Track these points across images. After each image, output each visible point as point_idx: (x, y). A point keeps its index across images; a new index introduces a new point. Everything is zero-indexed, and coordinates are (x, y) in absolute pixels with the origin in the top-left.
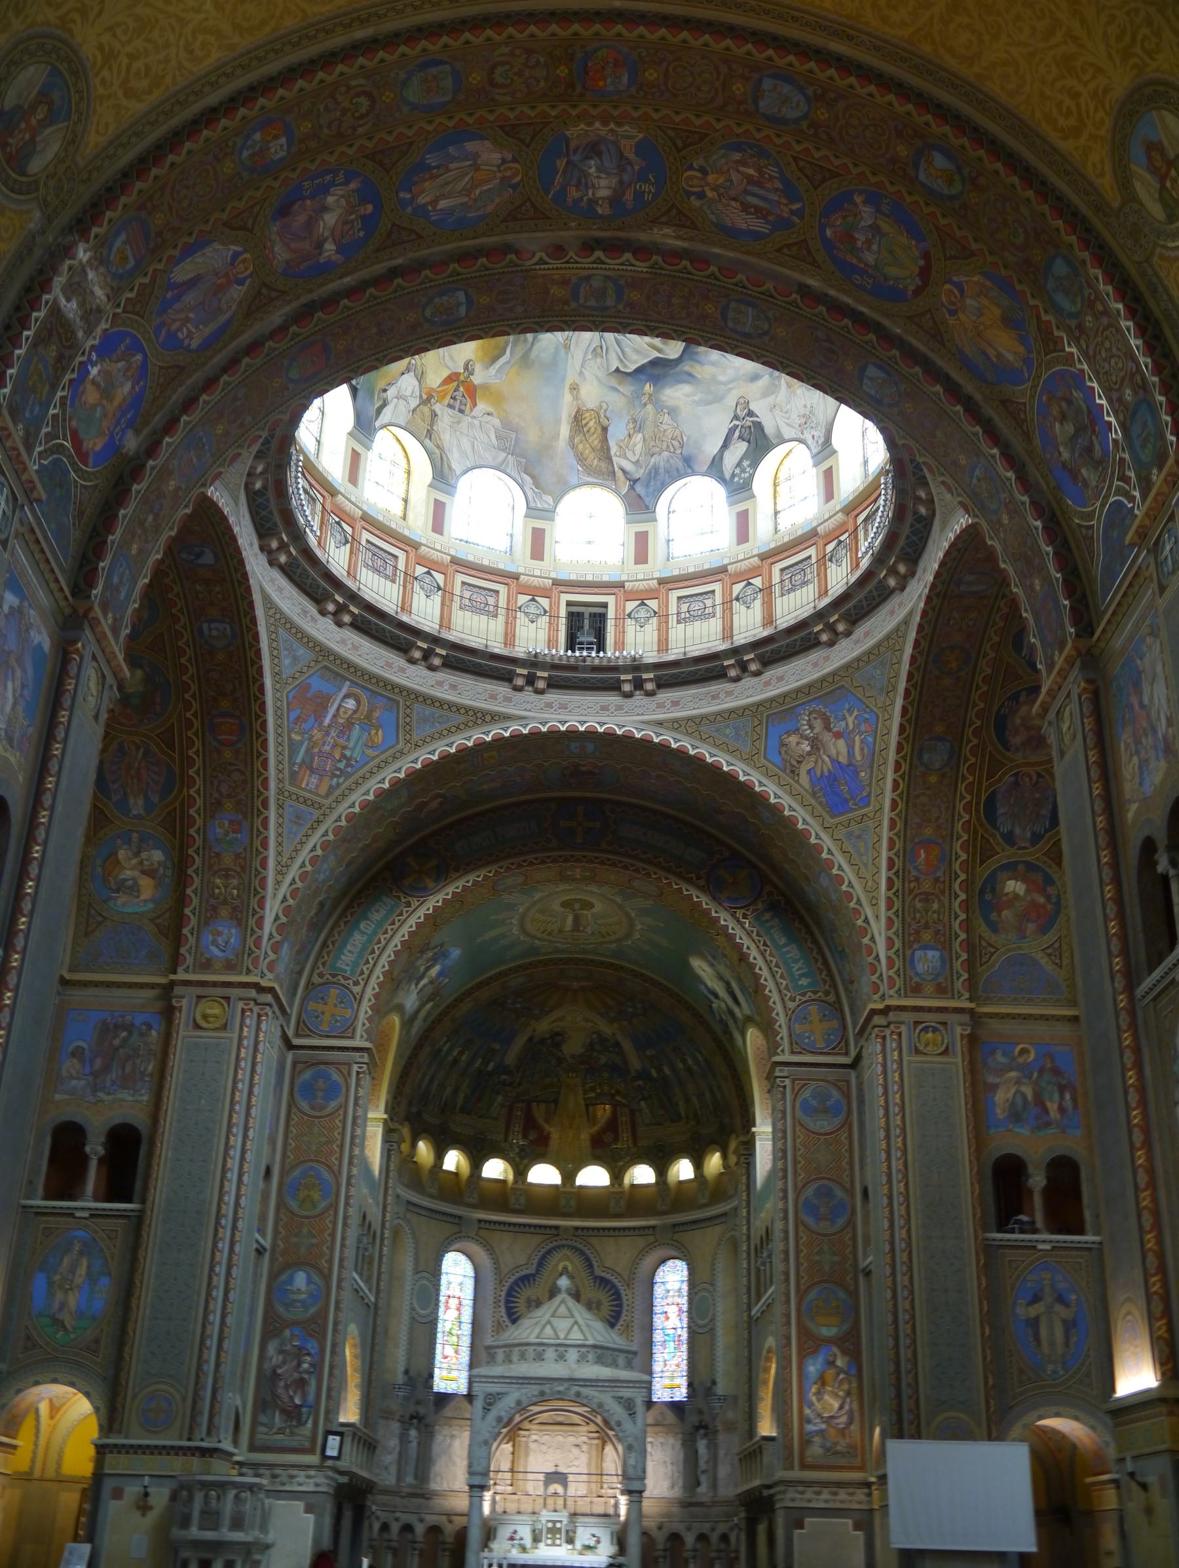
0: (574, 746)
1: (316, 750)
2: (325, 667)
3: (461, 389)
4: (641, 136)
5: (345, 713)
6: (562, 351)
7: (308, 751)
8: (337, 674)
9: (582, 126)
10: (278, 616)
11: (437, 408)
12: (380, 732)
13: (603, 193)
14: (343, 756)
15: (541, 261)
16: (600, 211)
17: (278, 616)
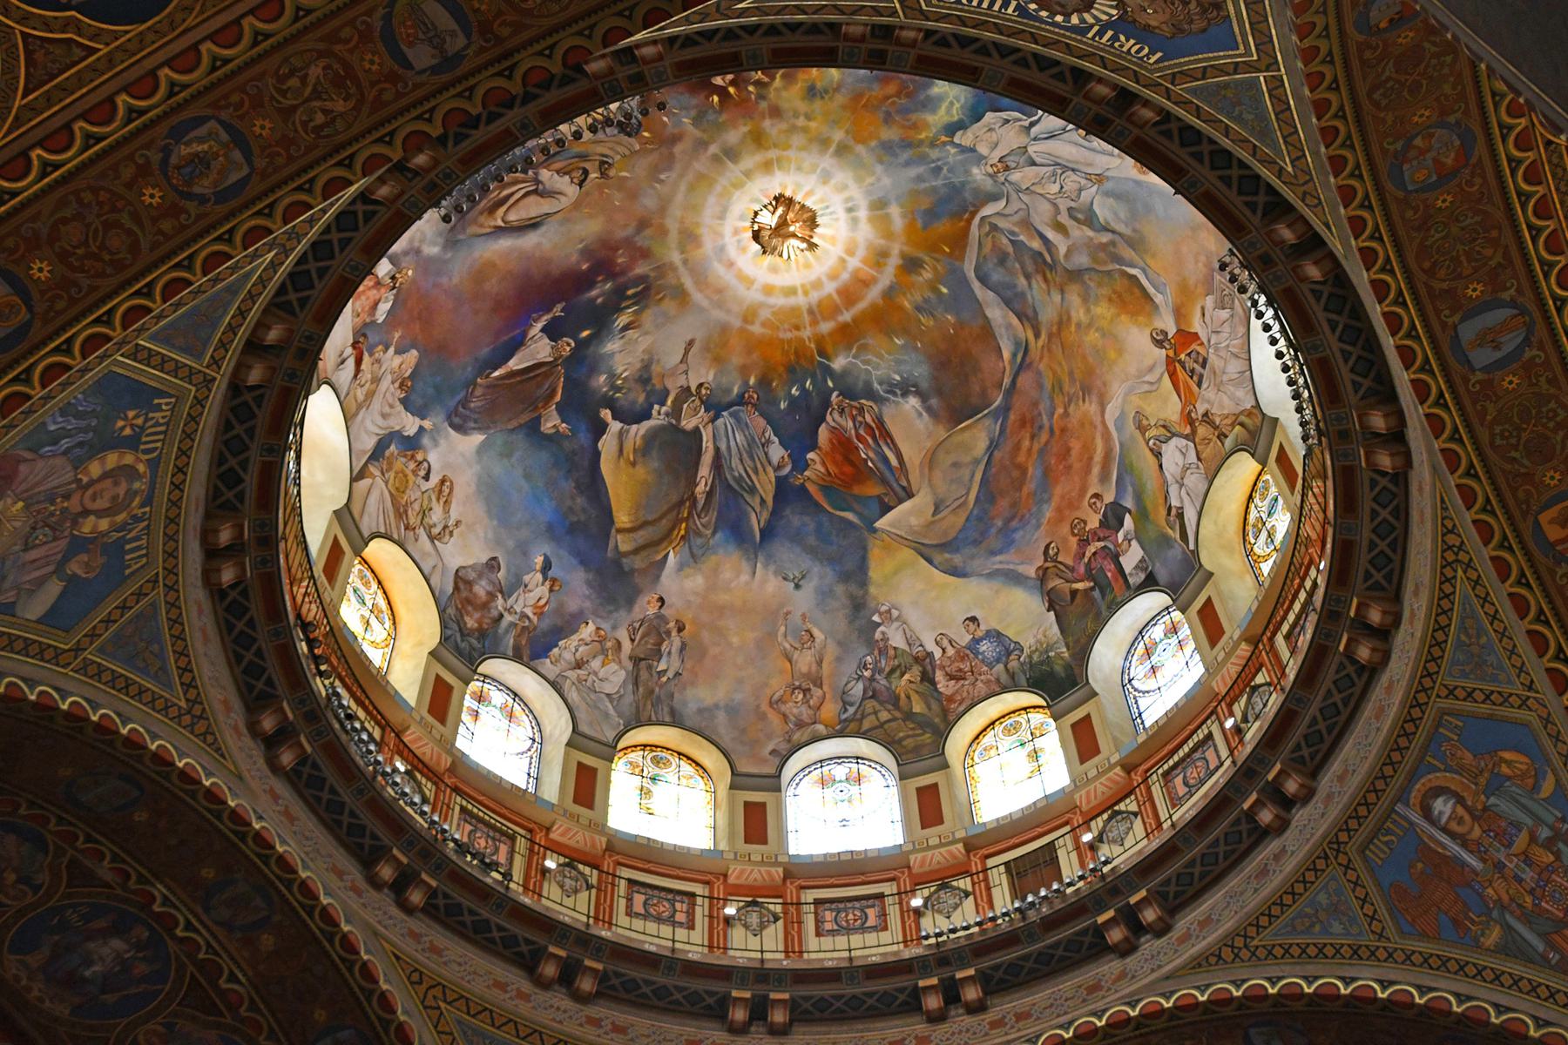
0: (1483, 357)
1: (1529, 899)
2: (1362, 851)
3: (1183, 356)
4: (12, 957)
5: (1460, 821)
6: (1108, 185)
7: (1526, 919)
8: (1378, 830)
9: (47, 1004)
10: (1239, 942)
11: (1201, 409)
12: (1507, 755)
13: (117, 944)
14: (1549, 844)
15: (233, 978)
16: (147, 934)
17: (1239, 942)
